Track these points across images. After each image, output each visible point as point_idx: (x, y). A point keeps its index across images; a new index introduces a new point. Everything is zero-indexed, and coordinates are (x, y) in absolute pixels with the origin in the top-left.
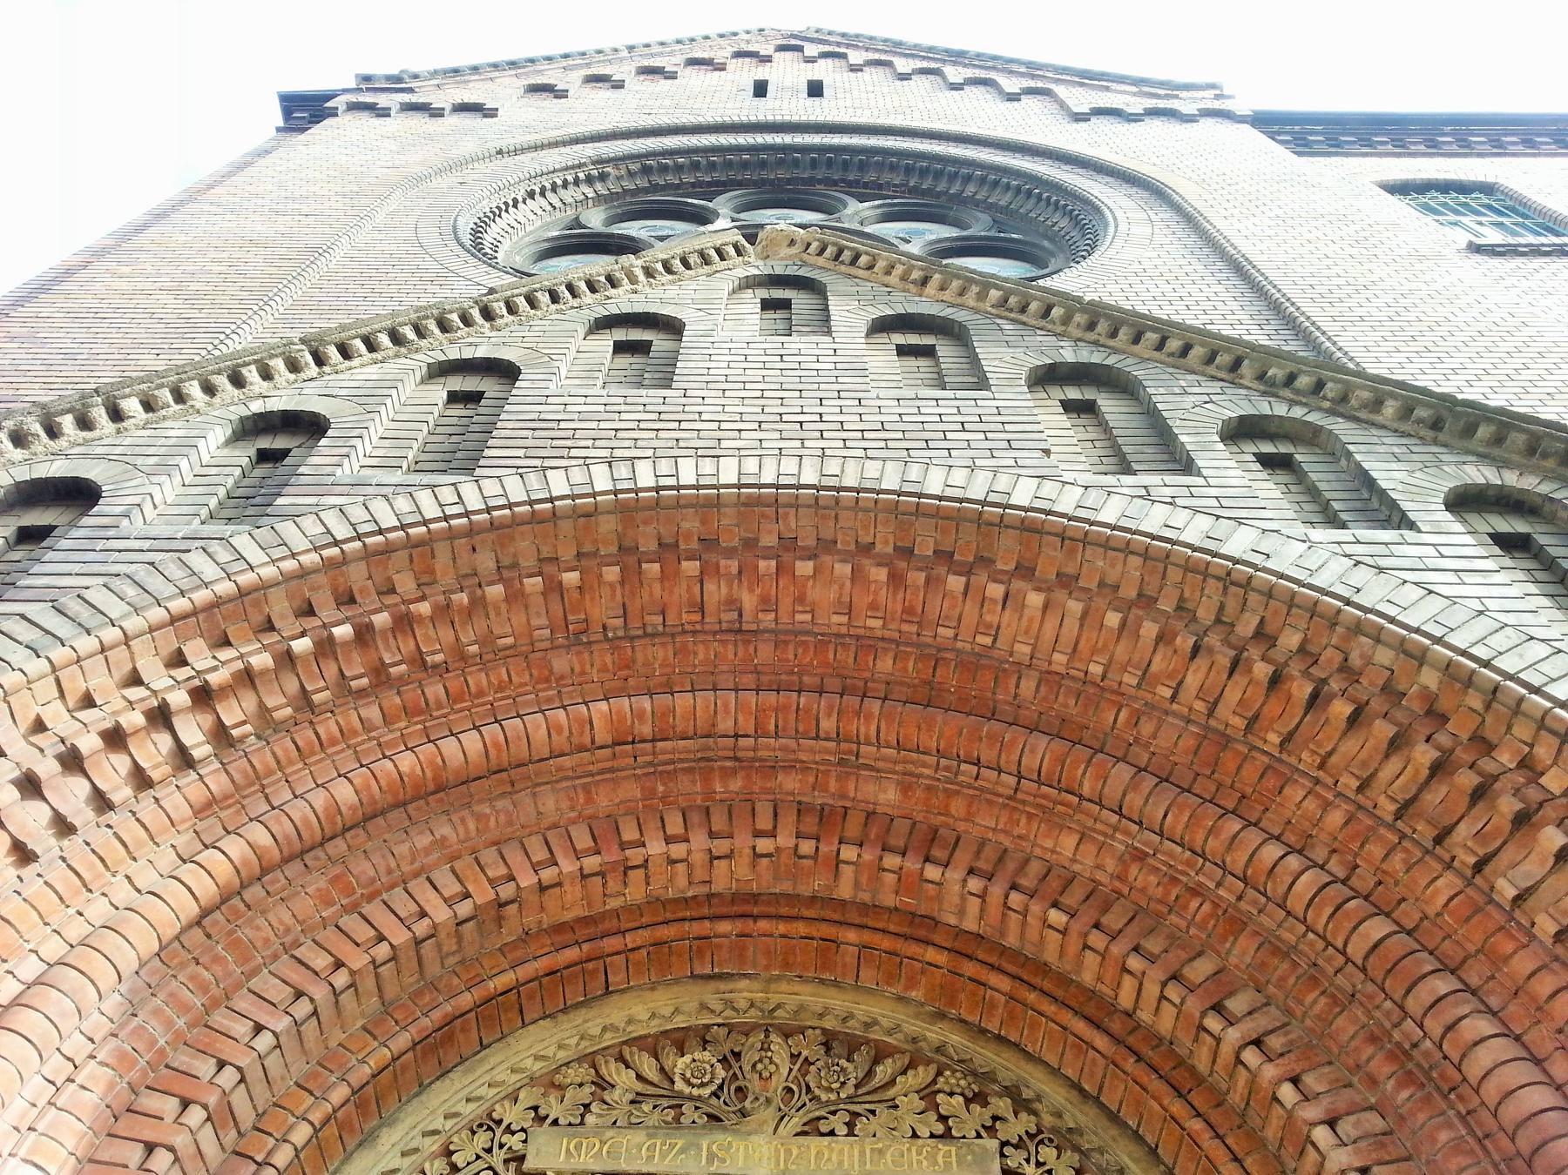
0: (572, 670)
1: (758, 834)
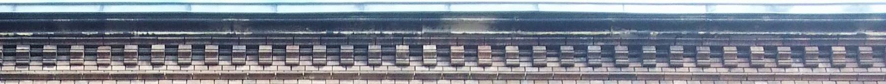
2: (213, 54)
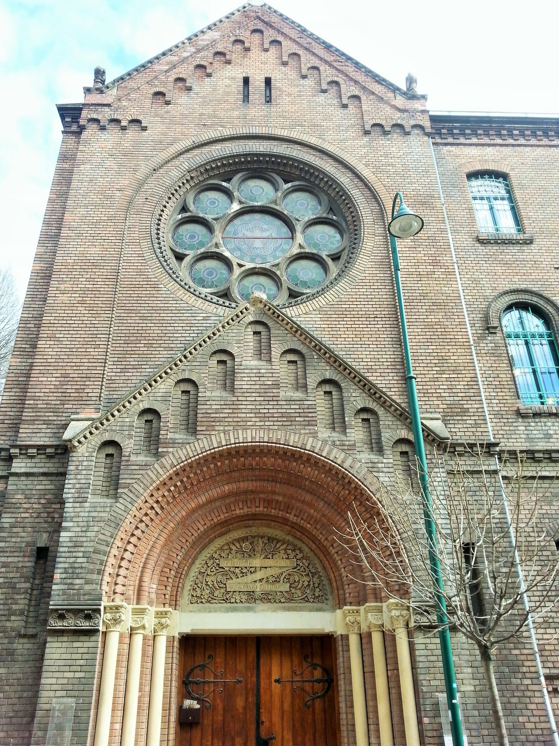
1: (256, 507)
2: (540, 136)
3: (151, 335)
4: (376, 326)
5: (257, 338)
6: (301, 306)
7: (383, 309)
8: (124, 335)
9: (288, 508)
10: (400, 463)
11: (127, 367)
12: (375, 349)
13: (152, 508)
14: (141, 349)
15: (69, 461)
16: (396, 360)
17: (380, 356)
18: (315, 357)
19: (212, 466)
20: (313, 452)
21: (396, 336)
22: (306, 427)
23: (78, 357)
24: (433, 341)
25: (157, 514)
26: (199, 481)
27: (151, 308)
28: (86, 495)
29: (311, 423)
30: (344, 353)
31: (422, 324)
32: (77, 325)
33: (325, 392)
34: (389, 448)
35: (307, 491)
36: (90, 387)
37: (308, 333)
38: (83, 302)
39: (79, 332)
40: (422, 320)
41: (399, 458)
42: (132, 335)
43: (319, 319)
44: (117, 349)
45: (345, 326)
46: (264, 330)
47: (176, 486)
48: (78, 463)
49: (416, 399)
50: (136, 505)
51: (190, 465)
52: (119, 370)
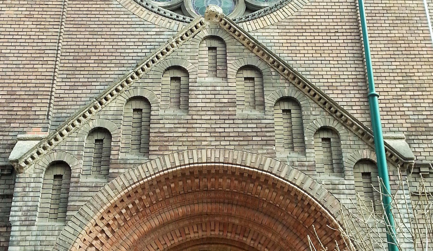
0: (174, 201)
1: (212, 231)
3: (101, 51)
4: (337, 41)
5: (213, 54)
6: (258, 20)
7: (344, 24)
8: (73, 51)
9: (244, 232)
10: (361, 184)
11: (76, 84)
12: (335, 66)
13: (103, 231)
14: (91, 65)
15: (15, 182)
16: (358, 77)
17: (342, 73)
18: (274, 73)
19: (165, 188)
20: (271, 173)
21: (358, 52)
22: (264, 147)
23: (25, 74)
24: (397, 56)
25: (108, 237)
26: (152, 204)
27: (101, 23)
28: (33, 218)
29: (269, 142)
30: (303, 69)
31: (385, 39)
32: (24, 41)
33: (284, 111)
34: (350, 169)
35: (265, 214)
36: (38, 105)
37: (266, 49)
38: (30, 16)
39: (26, 48)
40: (385, 35)
41: (361, 179)
42: (81, 51)
43: (277, 34)
44: (65, 65)
45: (305, 41)
46: (220, 45)
47: (127, 208)
48: (25, 185)
49: (379, 118)
50: (86, 228)
51: (143, 187)
52: (68, 88)
